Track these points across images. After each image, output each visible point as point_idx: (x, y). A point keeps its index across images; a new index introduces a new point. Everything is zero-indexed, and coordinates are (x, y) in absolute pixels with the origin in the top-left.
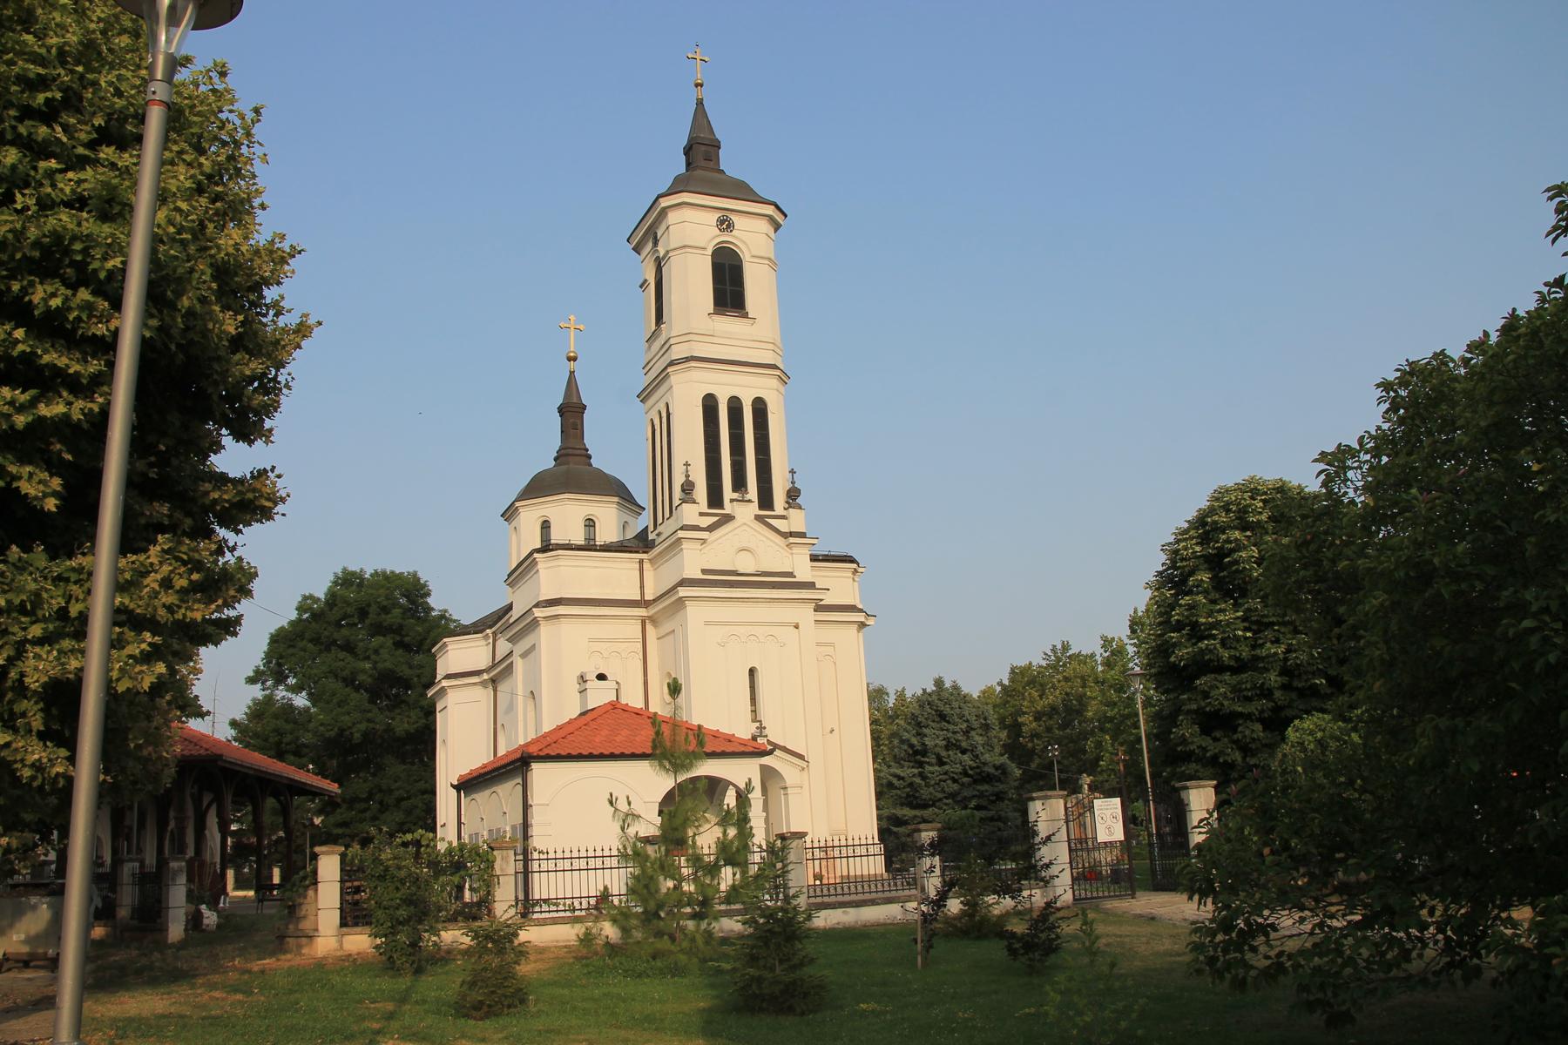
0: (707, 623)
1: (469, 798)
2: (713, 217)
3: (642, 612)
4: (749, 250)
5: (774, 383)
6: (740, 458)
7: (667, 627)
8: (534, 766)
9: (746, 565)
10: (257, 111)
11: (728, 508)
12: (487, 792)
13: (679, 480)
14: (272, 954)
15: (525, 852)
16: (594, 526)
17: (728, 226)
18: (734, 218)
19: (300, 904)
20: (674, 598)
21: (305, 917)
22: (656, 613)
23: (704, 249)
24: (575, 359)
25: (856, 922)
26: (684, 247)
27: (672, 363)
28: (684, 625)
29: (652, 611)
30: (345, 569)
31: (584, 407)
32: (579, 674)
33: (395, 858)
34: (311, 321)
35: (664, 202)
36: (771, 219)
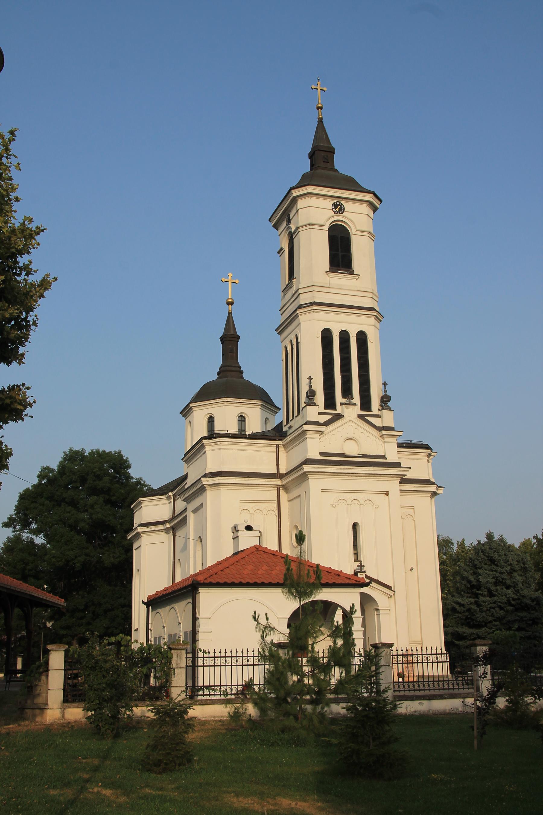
0: (323, 491)
1: (155, 612)
2: (329, 203)
3: (278, 482)
5: (372, 320)
6: (347, 374)
7: (295, 493)
8: (201, 590)
9: (351, 449)
10: (12, 133)
11: (339, 409)
12: (168, 608)
13: (304, 389)
14: (15, 721)
15: (193, 652)
16: (245, 421)
17: (340, 209)
18: (345, 204)
19: (36, 685)
20: (300, 473)
21: (39, 695)
22: (287, 483)
23: (323, 226)
24: (232, 303)
25: (429, 711)
26: (309, 224)
27: (300, 307)
28: (307, 492)
29: (285, 481)
31: (238, 337)
32: (233, 525)
33: (103, 654)
34: (50, 278)
35: (295, 193)
36: (371, 204)
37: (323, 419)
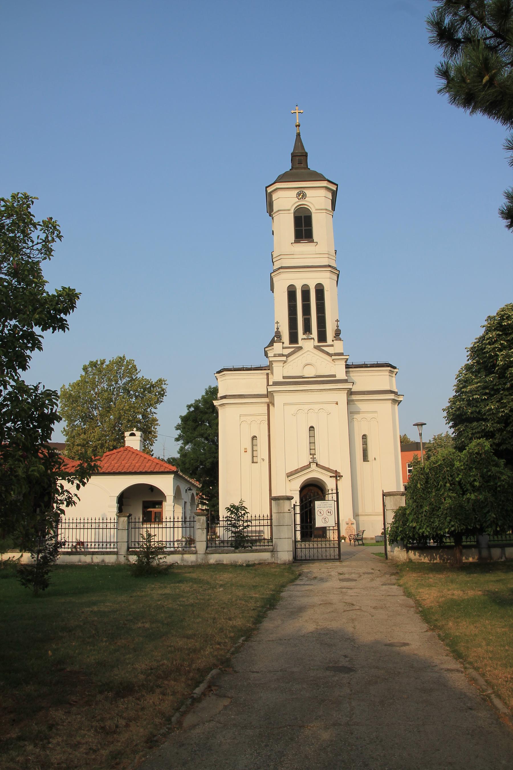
2: (295, 193)
4: (314, 206)
5: (328, 274)
9: (309, 372)
11: (301, 343)
18: (306, 191)
23: (289, 210)
27: (274, 271)
30: (210, 387)
37: (287, 352)
